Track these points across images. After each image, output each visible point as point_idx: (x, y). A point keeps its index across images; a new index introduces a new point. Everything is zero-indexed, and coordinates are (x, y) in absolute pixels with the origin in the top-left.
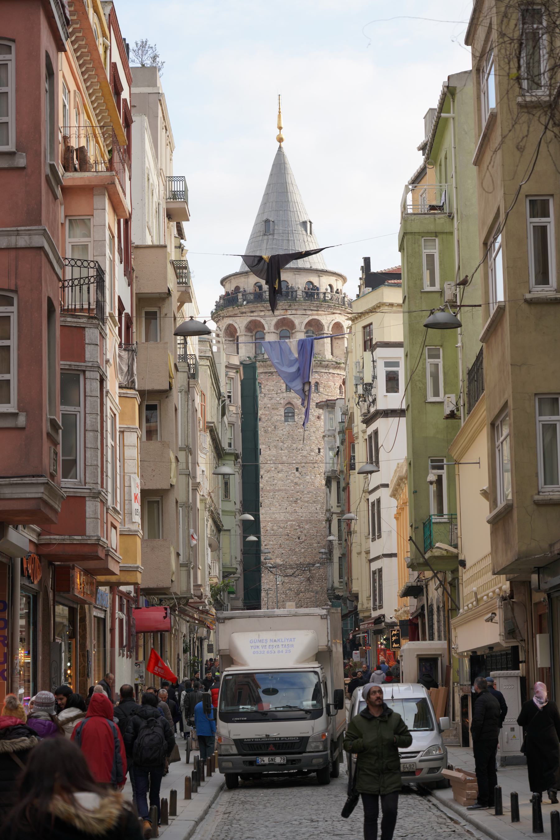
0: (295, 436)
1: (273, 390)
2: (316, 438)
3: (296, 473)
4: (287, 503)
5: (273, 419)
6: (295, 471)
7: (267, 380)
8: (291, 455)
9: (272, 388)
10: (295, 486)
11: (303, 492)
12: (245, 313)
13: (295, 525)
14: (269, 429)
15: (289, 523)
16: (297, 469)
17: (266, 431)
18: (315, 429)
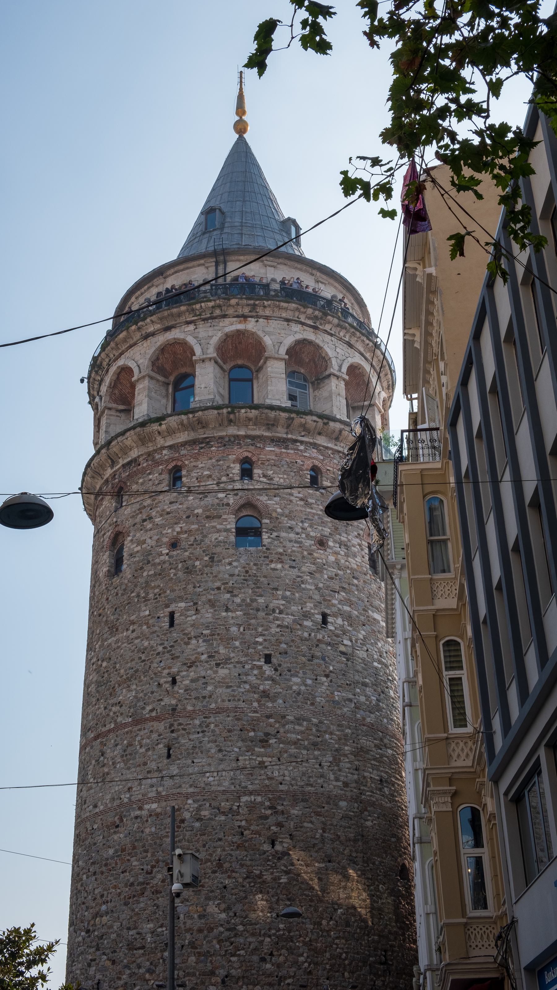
0: (262, 579)
1: (210, 476)
2: (318, 589)
3: (266, 667)
4: (240, 744)
5: (207, 541)
6: (262, 662)
7: (196, 457)
8: (253, 621)
9: (206, 473)
10: (263, 700)
11: (284, 717)
12: (153, 334)
13: (262, 803)
14: (197, 563)
15: (244, 799)
16: (268, 659)
17: (189, 571)
18: (313, 568)
